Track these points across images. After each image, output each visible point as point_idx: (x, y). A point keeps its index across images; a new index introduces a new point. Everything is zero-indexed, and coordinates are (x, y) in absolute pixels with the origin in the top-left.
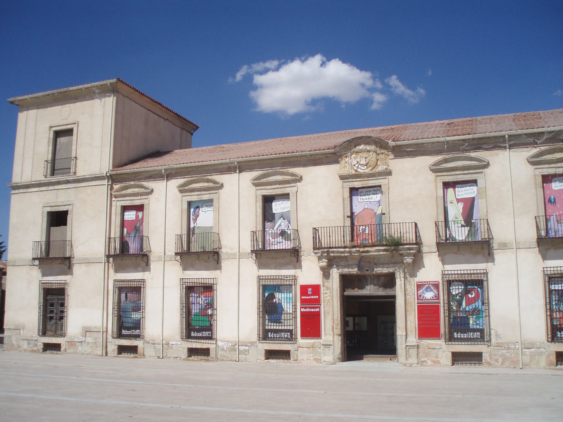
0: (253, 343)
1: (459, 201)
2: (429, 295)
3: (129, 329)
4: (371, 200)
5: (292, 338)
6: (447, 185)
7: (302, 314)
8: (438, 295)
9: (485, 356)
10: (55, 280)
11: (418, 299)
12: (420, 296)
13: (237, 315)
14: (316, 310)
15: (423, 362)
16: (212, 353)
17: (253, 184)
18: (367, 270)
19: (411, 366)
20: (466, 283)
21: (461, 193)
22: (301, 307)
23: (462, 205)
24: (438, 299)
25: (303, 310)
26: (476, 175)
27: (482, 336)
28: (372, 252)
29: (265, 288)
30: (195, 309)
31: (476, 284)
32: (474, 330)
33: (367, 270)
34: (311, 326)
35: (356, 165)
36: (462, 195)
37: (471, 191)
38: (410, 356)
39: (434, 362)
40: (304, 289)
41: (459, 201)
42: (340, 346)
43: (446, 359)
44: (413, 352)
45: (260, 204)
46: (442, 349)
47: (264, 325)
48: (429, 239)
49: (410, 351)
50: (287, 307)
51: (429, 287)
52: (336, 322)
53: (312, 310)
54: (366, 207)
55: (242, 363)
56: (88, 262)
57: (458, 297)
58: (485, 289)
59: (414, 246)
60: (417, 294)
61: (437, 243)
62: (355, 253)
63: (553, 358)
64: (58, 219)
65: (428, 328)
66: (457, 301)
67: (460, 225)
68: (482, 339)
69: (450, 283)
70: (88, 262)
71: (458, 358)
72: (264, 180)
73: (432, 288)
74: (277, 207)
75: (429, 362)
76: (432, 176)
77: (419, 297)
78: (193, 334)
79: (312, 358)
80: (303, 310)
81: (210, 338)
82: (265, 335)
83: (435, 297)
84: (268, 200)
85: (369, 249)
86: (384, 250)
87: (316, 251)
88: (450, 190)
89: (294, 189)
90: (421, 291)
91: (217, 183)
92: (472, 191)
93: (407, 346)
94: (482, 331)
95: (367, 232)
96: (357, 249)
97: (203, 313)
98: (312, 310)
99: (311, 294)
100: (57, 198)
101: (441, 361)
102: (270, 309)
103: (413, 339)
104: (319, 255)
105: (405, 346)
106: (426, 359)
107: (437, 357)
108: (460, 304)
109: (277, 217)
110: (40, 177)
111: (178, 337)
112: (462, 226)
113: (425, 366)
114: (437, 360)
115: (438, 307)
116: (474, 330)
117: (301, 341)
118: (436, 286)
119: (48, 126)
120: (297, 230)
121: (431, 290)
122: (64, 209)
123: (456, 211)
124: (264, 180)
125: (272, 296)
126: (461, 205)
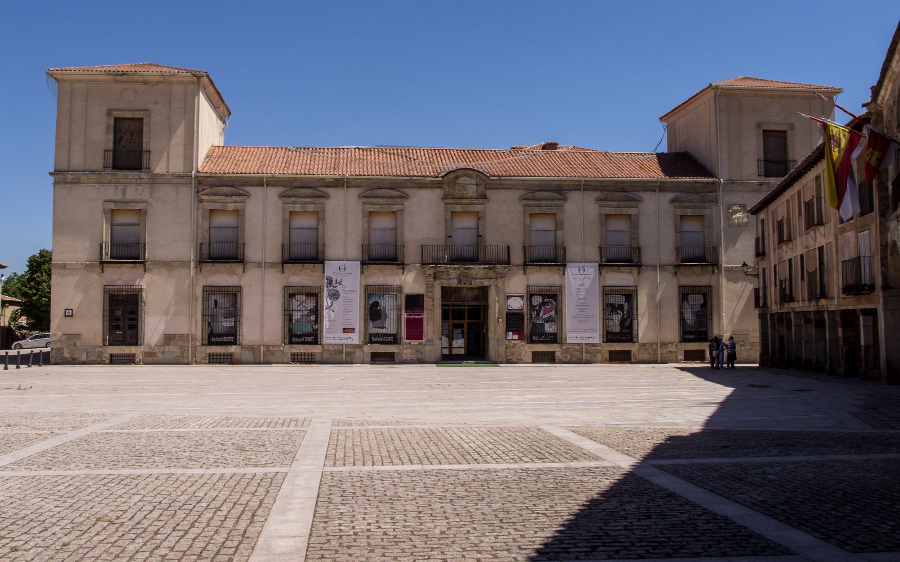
0: (359, 347)
3: (220, 335)
5: (395, 340)
7: (408, 321)
9: (558, 355)
13: (342, 319)
30: (297, 316)
34: (415, 329)
56: (168, 265)
70: (168, 265)
82: (371, 339)
99: (414, 302)
102: (374, 313)
108: (538, 314)
111: (279, 342)
125: (376, 304)
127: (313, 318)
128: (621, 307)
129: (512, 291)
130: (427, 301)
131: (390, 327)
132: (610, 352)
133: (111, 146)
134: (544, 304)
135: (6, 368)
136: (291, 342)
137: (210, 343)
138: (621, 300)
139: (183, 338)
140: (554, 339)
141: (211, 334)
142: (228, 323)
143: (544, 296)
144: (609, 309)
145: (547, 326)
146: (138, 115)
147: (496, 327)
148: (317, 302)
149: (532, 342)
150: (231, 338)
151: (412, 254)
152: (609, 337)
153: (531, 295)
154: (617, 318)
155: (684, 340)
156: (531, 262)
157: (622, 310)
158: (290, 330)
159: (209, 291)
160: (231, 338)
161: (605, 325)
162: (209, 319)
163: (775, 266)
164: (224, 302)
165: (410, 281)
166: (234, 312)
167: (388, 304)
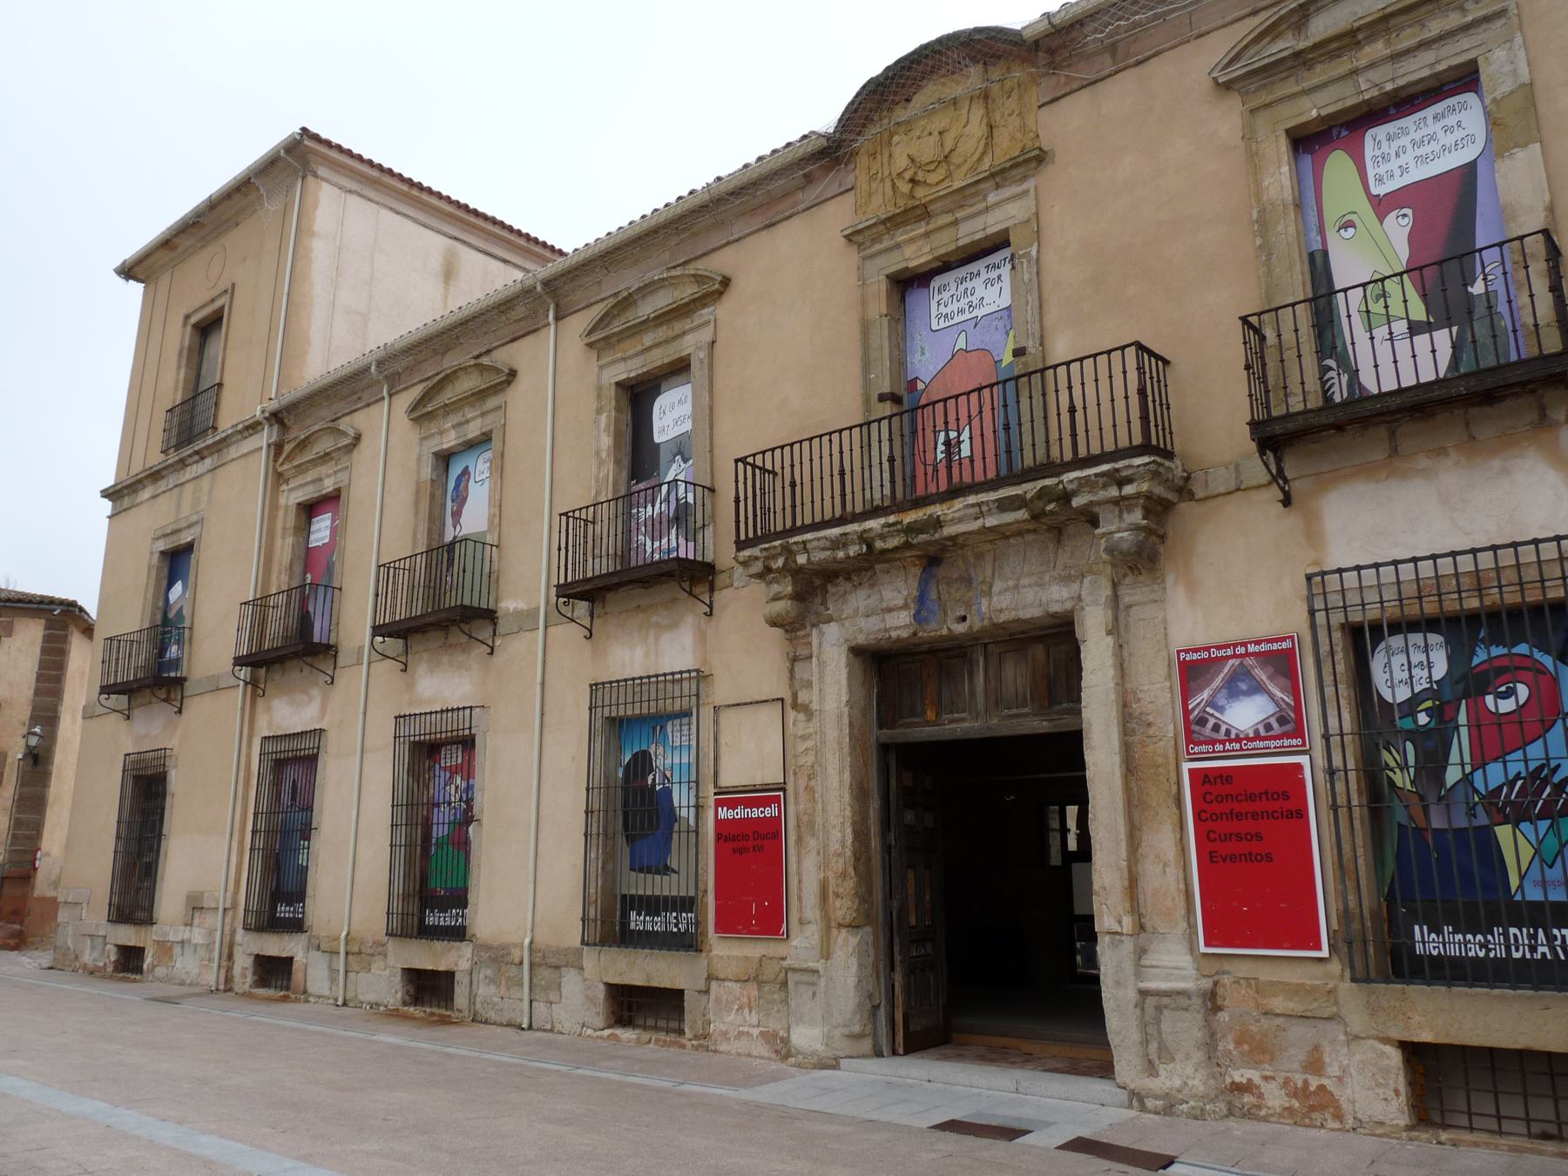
1: (1382, 206)
4: (979, 313)
6: (1309, 141)
8: (1297, 708)
11: (1189, 741)
12: (1202, 721)
14: (769, 812)
15: (1238, 1088)
17: (590, 345)
18: (964, 619)
19: (1169, 1110)
20: (1458, 628)
21: (1394, 164)
22: (719, 803)
23: (1407, 222)
24: (1298, 732)
25: (724, 813)
26: (1465, 42)
28: (954, 521)
29: (618, 727)
33: (964, 619)
35: (908, 175)
36: (1404, 170)
37: (1449, 140)
38: (1166, 1054)
39: (1302, 1093)
41: (1382, 206)
42: (852, 981)
43: (1372, 1085)
44: (1185, 1028)
47: (609, 876)
48: (1215, 416)
49: (1166, 1026)
51: (1242, 674)
52: (838, 865)
53: (756, 813)
54: (961, 344)
55: (539, 1034)
57: (1423, 719)
59: (1138, 461)
60: (1187, 713)
61: (1254, 424)
62: (883, 537)
66: (1416, 735)
67: (1400, 327)
69: (1362, 639)
72: (616, 326)
73: (1261, 675)
74: (671, 415)
75: (1275, 1097)
76: (1227, 119)
77: (1195, 729)
79: (755, 1032)
80: (724, 813)
82: (614, 924)
83: (1282, 721)
85: (937, 510)
86: (1004, 505)
87: (746, 553)
88: (1338, 164)
89: (705, 335)
90: (1205, 695)
91: (498, 371)
92: (1458, 134)
93: (1144, 993)
95: (965, 450)
96: (892, 519)
98: (756, 813)
101: (1343, 1096)
103: (1176, 961)
104: (758, 567)
105: (1131, 995)
106: (1255, 1075)
107: (1315, 1064)
109: (664, 455)
112: (1414, 329)
113: (1249, 1114)
114: (1314, 1083)
117: (726, 951)
118: (1283, 663)
119: (181, 318)
120: (712, 490)
121: (1257, 688)
123: (1372, 250)
124: (616, 326)
125: (642, 762)
126: (1399, 227)
134: (1469, 683)
143: (1458, 628)
145: (1515, 845)
153: (1362, 639)
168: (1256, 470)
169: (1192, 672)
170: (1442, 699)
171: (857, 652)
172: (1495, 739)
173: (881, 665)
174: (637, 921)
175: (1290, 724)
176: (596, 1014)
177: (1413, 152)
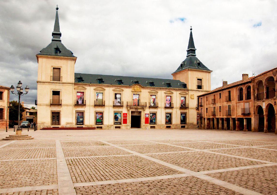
0: (112, 125)
1: (152, 99)
2: (147, 116)
3: (79, 123)
5: (120, 124)
7: (123, 119)
9: (156, 127)
10: (56, 109)
13: (109, 119)
16: (103, 128)
20: (153, 114)
27: (155, 123)
30: (97, 118)
31: (154, 114)
32: (154, 122)
34: (125, 121)
40: (124, 114)
45: (114, 95)
46: (149, 126)
48: (148, 105)
50: (119, 117)
56: (67, 105)
58: (156, 115)
63: (166, 127)
64: (56, 93)
65: (146, 122)
68: (155, 124)
70: (67, 105)
71: (151, 127)
76: (148, 93)
77: (145, 116)
78: (97, 124)
81: (102, 124)
82: (115, 123)
84: (116, 94)
94: (155, 122)
97: (99, 118)
99: (125, 115)
100: (57, 87)
102: (116, 118)
103: (144, 124)
108: (152, 118)
109: (117, 98)
110: (49, 80)
115: (148, 118)
116: (154, 122)
117: (123, 124)
118: (148, 114)
122: (59, 91)
123: (152, 101)
125: (116, 115)
126: (153, 99)
127: (101, 118)
128: (169, 116)
129: (146, 113)
130: (128, 115)
131: (119, 121)
132: (167, 126)
133: (52, 75)
134: (153, 115)
135: (28, 131)
136: (96, 124)
137: (77, 124)
138: (169, 115)
139: (72, 123)
140: (155, 123)
141: (77, 122)
142: (81, 119)
144: (167, 117)
145: (153, 120)
146: (60, 67)
147: (143, 120)
148: (102, 115)
149: (150, 124)
150: (82, 123)
151: (125, 104)
152: (166, 123)
154: (168, 119)
155: (181, 124)
156: (150, 107)
157: (169, 117)
158: (96, 121)
159: (77, 112)
160: (82, 123)
161: (166, 120)
162: (77, 119)
163: (207, 109)
164: (80, 114)
165: (124, 110)
166: (83, 117)
167: (118, 115)
168: (148, 107)
169: (146, 114)
170: (152, 116)
171: (131, 111)
172: (153, 117)
173: (132, 112)
174: (115, 123)
175: (149, 116)
176: (114, 128)
177: (154, 97)
